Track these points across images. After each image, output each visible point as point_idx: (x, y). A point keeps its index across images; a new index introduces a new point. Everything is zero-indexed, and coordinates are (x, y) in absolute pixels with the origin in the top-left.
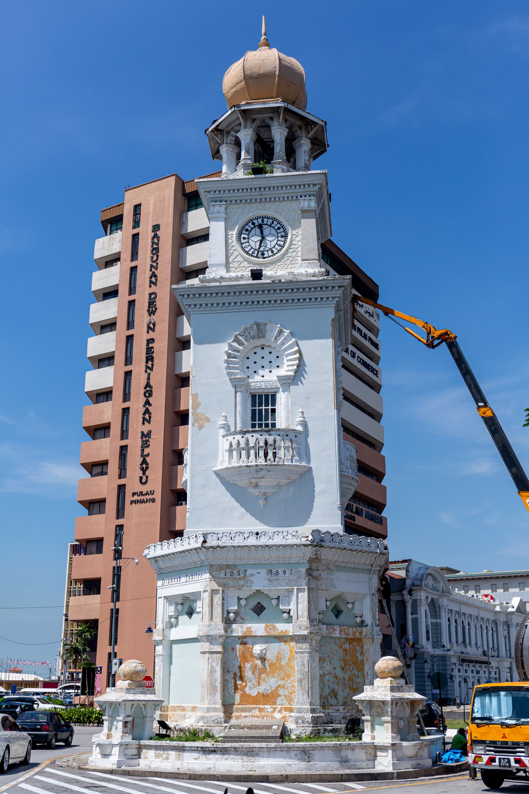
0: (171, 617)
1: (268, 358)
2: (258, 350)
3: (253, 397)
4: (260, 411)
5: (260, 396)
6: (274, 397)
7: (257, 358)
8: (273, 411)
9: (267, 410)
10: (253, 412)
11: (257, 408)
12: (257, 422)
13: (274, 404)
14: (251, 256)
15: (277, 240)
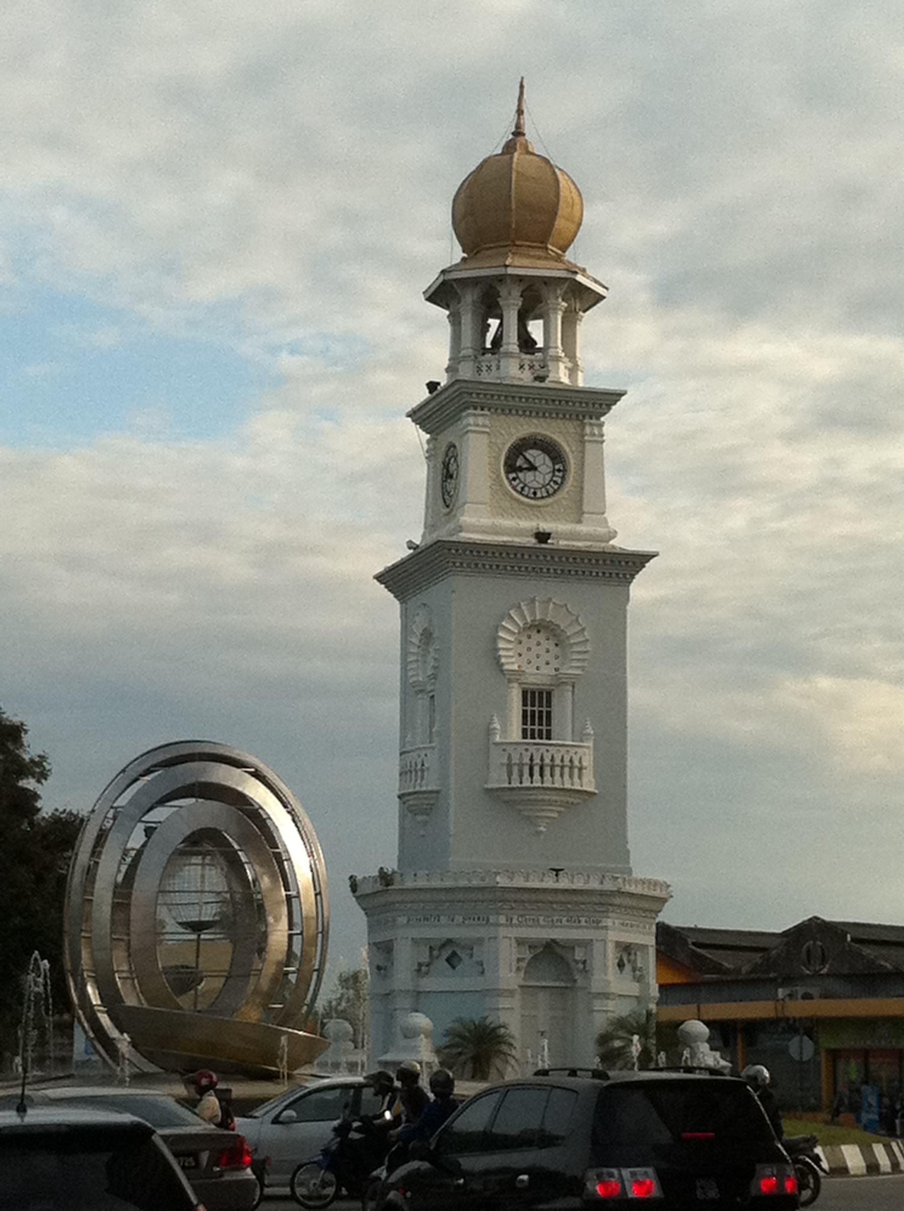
0: (420, 965)
1: (545, 644)
2: (534, 634)
3: (525, 693)
4: (533, 712)
5: (533, 693)
6: (549, 694)
7: (533, 642)
8: (549, 714)
9: (541, 712)
10: (525, 713)
11: (529, 708)
12: (529, 727)
13: (549, 704)
14: (521, 493)
15: (551, 475)
